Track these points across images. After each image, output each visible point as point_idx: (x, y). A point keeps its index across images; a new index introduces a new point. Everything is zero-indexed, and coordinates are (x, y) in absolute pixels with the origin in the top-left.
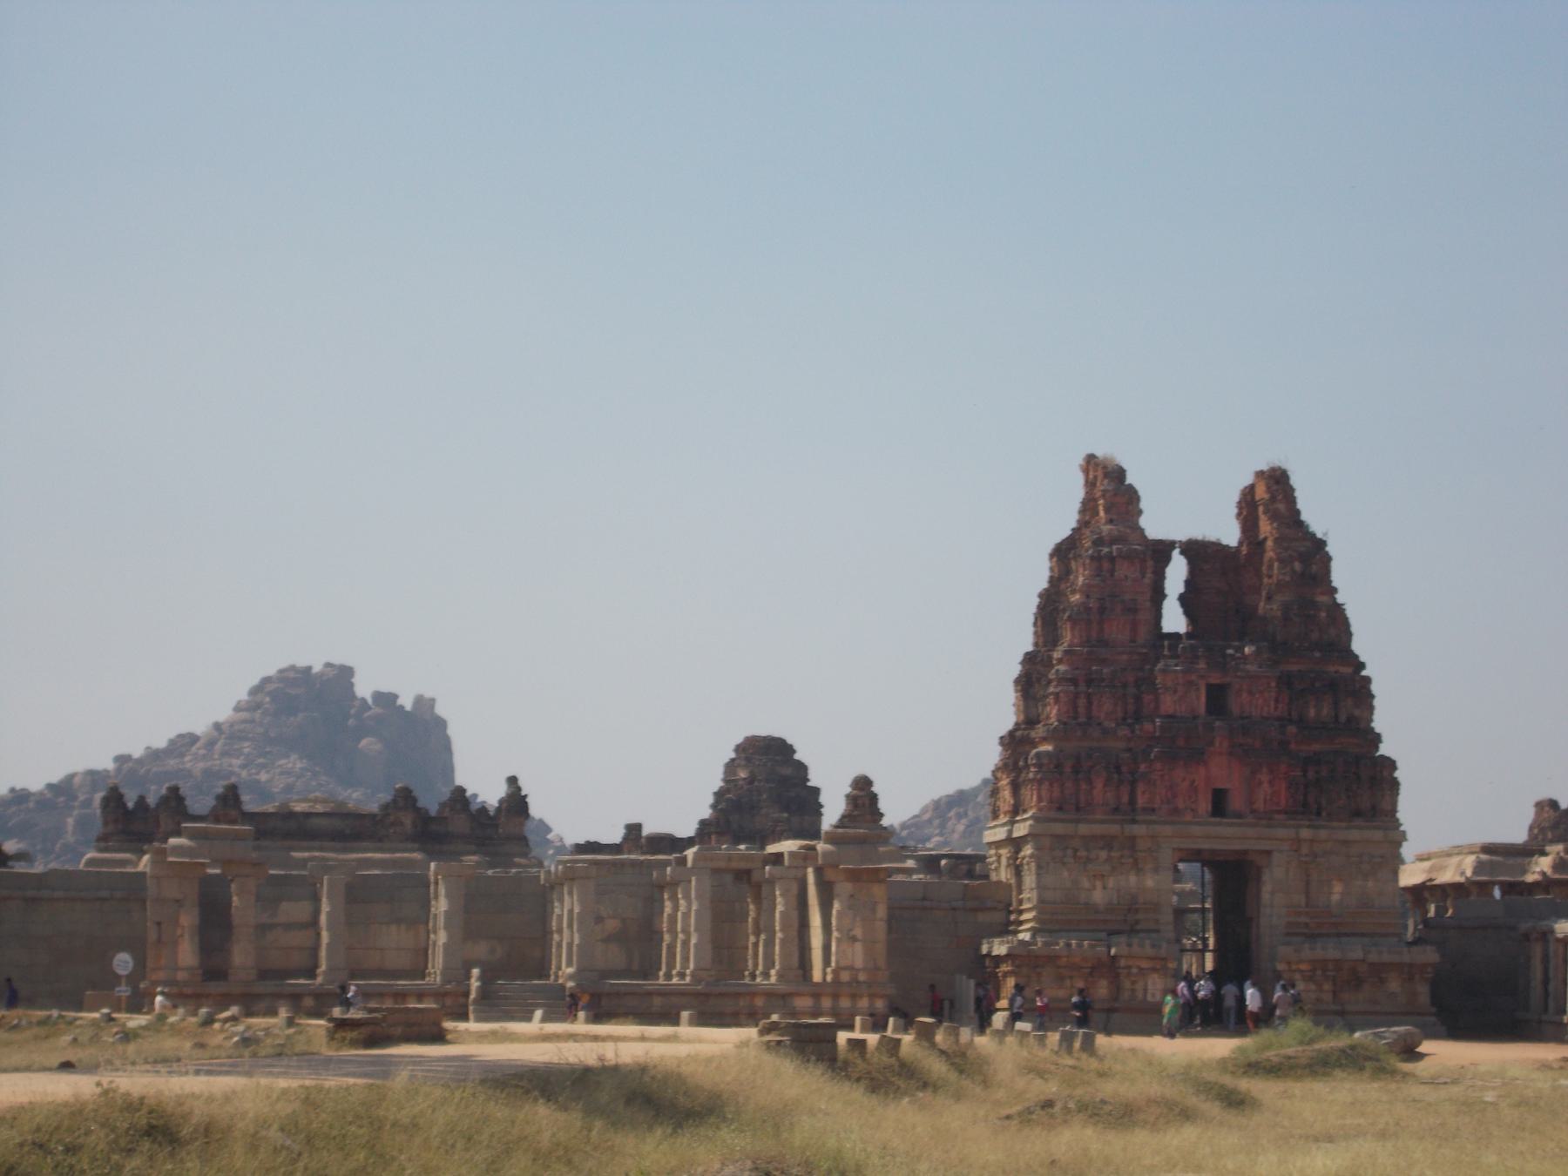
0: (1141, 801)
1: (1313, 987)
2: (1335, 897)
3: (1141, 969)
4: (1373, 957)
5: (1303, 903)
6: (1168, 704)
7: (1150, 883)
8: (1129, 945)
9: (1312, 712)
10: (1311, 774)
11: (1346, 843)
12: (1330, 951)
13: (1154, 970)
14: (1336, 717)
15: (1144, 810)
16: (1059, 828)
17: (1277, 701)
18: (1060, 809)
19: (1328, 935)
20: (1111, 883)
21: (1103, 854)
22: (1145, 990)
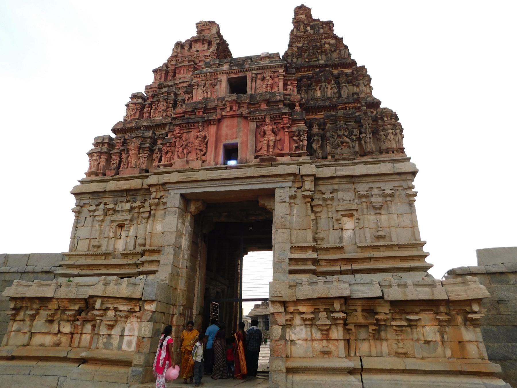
0: (163, 162)
1: (317, 335)
2: (347, 234)
3: (116, 310)
4: (394, 294)
5: (310, 237)
6: (198, 95)
7: (159, 228)
8: (106, 284)
9: (319, 94)
10: (315, 129)
11: (353, 178)
12: (339, 287)
13: (131, 312)
14: (339, 92)
15: (165, 166)
16: (94, 187)
17: (285, 85)
18: (104, 175)
19: (341, 273)
20: (132, 232)
21: (127, 206)
22: (122, 336)
